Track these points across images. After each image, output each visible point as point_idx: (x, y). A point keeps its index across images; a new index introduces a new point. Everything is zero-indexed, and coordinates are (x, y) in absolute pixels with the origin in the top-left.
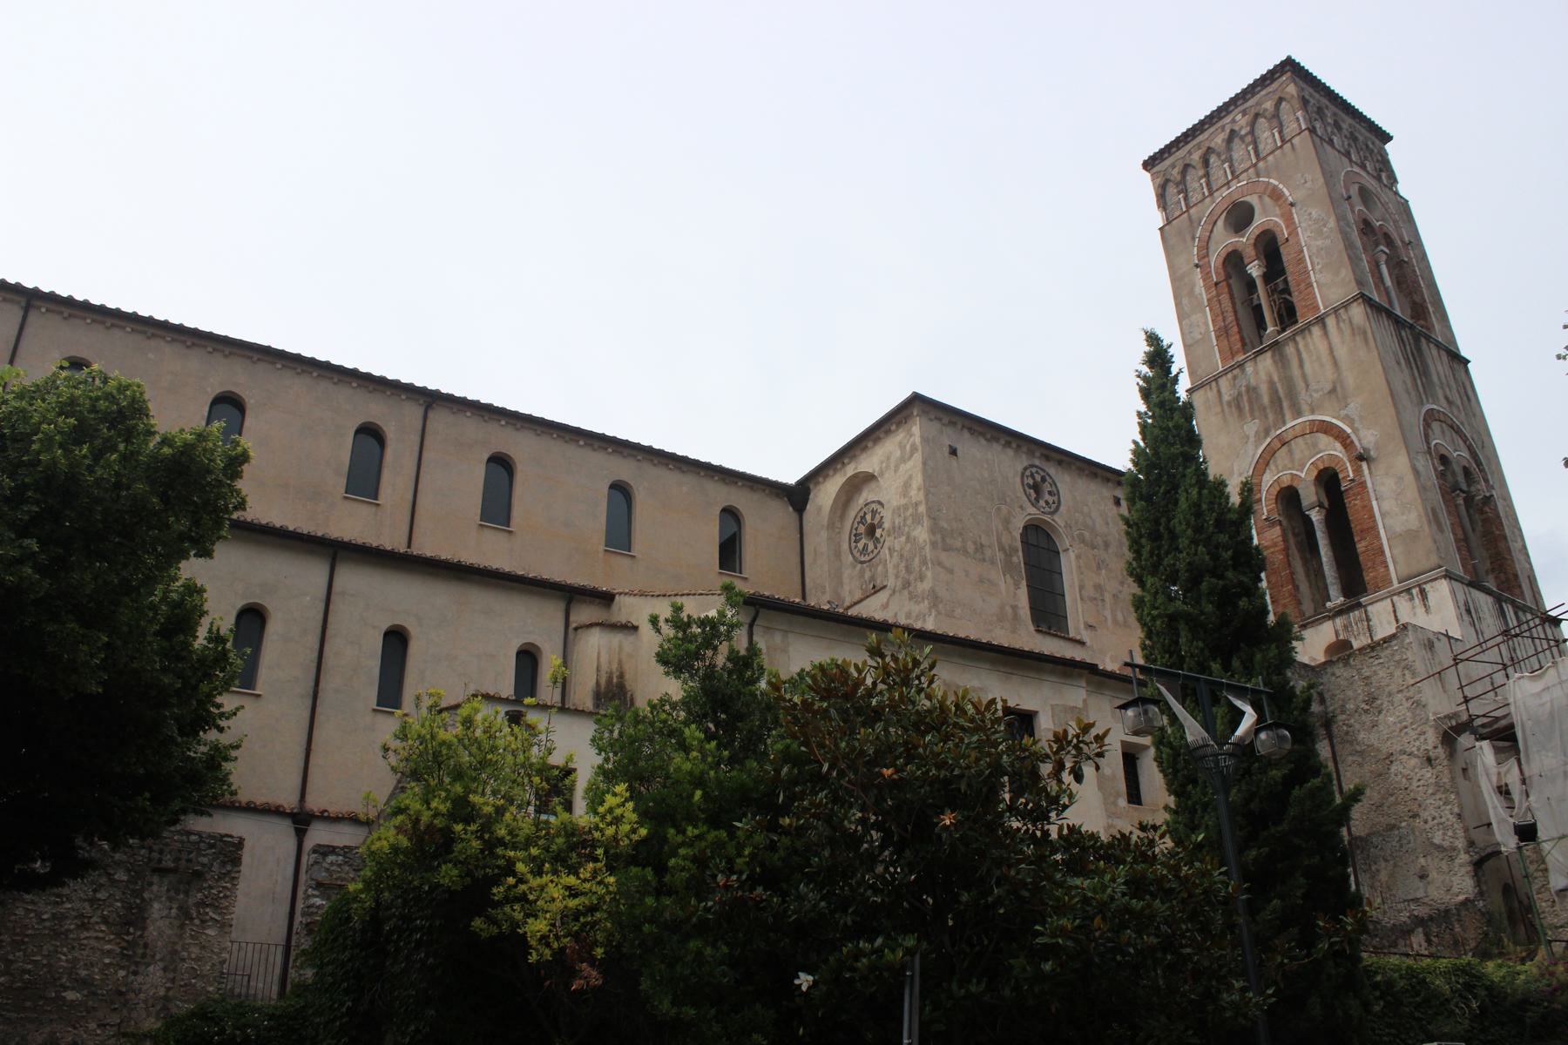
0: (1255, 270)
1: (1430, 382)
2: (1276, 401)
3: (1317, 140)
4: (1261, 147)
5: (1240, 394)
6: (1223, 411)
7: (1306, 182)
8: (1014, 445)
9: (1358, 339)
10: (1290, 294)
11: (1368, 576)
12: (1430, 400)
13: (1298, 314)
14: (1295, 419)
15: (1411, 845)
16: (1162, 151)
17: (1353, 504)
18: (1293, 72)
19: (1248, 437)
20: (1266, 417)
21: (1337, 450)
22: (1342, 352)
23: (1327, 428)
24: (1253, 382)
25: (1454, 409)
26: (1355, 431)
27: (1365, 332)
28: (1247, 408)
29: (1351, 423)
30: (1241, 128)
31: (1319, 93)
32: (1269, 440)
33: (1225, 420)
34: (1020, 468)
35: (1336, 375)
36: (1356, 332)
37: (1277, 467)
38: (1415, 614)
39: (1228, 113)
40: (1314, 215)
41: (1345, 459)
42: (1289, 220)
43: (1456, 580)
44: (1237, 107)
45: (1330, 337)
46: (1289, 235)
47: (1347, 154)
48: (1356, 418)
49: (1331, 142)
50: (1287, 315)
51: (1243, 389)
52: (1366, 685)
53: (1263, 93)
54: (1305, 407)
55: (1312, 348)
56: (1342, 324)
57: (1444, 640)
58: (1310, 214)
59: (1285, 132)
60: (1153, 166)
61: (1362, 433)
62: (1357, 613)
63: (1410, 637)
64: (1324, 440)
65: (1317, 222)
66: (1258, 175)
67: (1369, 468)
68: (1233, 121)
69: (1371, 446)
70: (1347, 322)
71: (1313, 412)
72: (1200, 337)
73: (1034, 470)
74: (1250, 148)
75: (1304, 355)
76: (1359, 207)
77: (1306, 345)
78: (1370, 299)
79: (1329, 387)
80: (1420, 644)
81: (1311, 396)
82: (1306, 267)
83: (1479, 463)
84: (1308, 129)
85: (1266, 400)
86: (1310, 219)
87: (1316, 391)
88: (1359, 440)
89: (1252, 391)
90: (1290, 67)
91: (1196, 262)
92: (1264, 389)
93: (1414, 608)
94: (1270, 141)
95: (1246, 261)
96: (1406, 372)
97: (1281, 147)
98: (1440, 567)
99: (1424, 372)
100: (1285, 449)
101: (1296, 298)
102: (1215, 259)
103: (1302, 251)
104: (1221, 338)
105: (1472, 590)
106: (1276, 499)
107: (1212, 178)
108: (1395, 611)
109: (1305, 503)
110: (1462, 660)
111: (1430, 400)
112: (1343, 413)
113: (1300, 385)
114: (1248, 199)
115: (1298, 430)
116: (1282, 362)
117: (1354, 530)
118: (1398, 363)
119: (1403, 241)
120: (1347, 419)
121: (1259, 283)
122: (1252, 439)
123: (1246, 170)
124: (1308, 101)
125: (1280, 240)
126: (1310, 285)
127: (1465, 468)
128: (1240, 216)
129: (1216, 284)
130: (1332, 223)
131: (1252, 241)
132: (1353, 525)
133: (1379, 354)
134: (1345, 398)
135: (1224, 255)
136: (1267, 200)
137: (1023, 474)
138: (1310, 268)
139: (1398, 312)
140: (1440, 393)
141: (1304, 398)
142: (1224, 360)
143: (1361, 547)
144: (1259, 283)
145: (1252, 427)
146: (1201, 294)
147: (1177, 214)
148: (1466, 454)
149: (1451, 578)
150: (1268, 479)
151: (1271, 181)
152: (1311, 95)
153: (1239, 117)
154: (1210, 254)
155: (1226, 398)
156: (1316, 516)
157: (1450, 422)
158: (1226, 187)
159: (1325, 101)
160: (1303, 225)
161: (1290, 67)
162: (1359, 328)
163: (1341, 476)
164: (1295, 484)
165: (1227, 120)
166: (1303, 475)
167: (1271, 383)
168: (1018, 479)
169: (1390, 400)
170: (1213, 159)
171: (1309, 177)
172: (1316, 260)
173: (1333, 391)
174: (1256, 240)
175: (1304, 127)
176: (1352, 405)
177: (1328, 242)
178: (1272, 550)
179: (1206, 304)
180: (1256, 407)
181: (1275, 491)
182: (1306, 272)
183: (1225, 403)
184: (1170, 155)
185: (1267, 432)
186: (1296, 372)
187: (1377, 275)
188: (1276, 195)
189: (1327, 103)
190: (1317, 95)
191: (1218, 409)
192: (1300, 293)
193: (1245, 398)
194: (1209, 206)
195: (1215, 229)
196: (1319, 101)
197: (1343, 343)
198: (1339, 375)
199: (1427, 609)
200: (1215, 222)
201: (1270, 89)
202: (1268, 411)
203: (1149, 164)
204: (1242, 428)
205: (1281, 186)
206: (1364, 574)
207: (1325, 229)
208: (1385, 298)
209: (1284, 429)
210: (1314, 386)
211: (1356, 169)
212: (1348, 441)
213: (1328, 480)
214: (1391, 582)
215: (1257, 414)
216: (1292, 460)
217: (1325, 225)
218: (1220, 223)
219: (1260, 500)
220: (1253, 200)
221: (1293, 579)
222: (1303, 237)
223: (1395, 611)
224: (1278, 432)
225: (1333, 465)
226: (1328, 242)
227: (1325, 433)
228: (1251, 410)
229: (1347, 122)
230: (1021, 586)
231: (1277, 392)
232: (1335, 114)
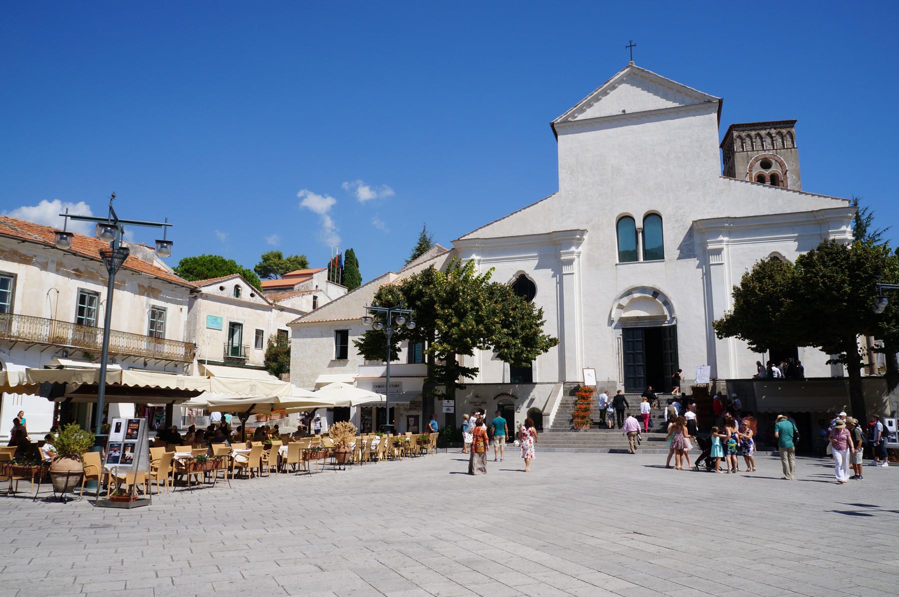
30: (773, 133)
65: (794, 180)
66: (777, 154)
102: (754, 174)
136: (778, 164)
158: (763, 151)
188: (782, 165)
194: (755, 155)
205: (784, 162)
220: (773, 161)
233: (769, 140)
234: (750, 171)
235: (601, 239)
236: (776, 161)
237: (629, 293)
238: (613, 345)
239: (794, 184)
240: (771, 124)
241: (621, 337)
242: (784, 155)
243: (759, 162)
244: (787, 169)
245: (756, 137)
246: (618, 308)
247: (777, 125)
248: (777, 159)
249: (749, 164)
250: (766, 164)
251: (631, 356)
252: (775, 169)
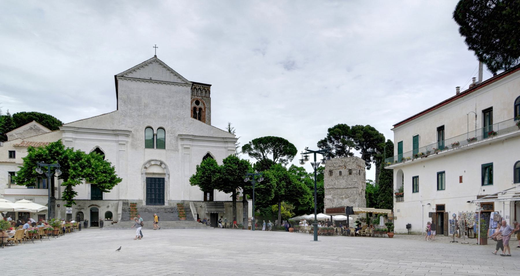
0: (198, 112)
4: (203, 94)
42: (205, 109)
53: (206, 86)
65: (208, 112)
68: (200, 86)
153: (201, 87)
165: (200, 85)
170: (195, 89)
188: (204, 105)
220: (201, 102)
233: (200, 92)
235: (138, 136)
237: (150, 161)
238: (142, 184)
241: (145, 181)
243: (195, 101)
245: (194, 90)
246: (145, 168)
247: (203, 85)
251: (149, 189)
252: (201, 105)
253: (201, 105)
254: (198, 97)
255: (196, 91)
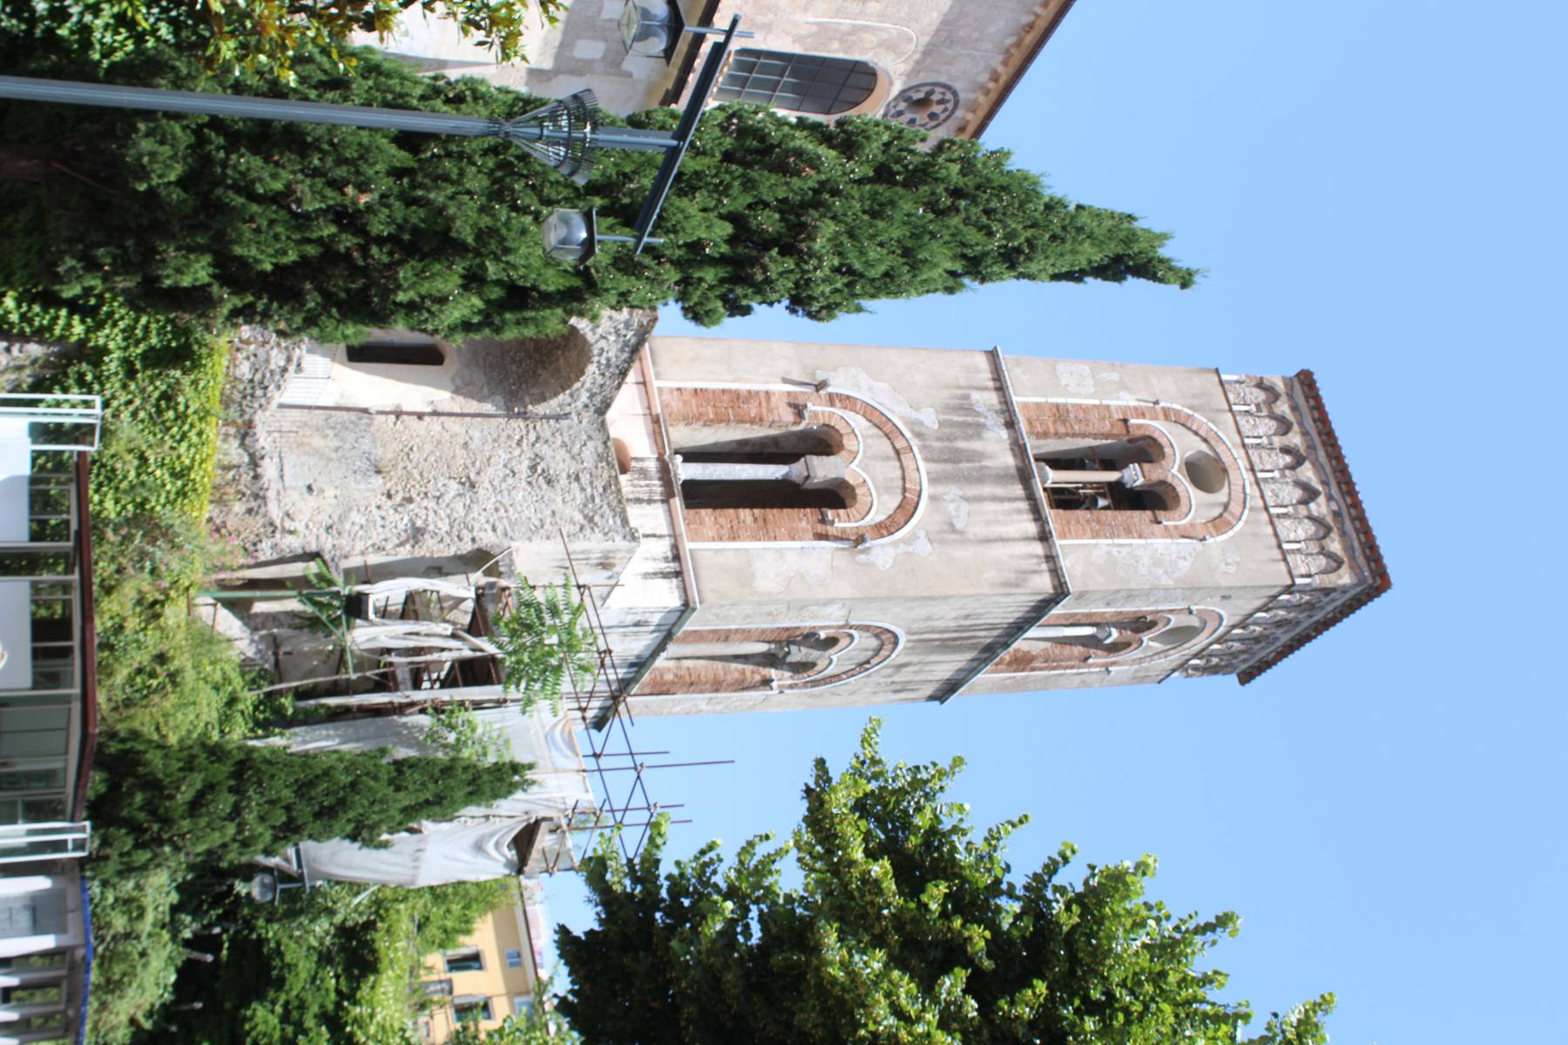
0: (1134, 476)
1: (933, 651)
2: (955, 457)
3: (1274, 592)
4: (1287, 523)
5: (978, 414)
6: (959, 387)
7: (1227, 564)
8: (991, 85)
9: (1012, 576)
10: (1088, 509)
11: (706, 514)
12: (911, 644)
13: (1061, 511)
14: (928, 473)
15: (353, 484)
16: (1317, 398)
17: (804, 518)
18: (1370, 587)
19: (917, 409)
20: (939, 439)
21: (875, 516)
22: (1000, 551)
23: (907, 509)
24: (987, 435)
25: (889, 671)
26: (895, 544)
27: (1017, 586)
28: (956, 418)
29: (907, 541)
31: (1333, 611)
32: (908, 435)
33: (947, 387)
34: (957, 86)
35: (971, 537)
36: (1022, 576)
37: (871, 437)
38: (647, 559)
39: (1343, 494)
40: (1182, 564)
41: (861, 523)
43: (680, 617)
44: (1348, 507)
45: (1022, 543)
46: (1166, 527)
47: (1243, 624)
48: (911, 549)
49: (1264, 608)
50: (1065, 499)
51: (982, 420)
52: (569, 476)
53: (1356, 544)
54: (940, 489)
55: (1015, 517)
56: (1035, 561)
57: (613, 582)
58: (1185, 559)
59: (1298, 557)
60: (1302, 383)
61: (891, 551)
62: (659, 489)
63: (620, 543)
64: (892, 502)
66: (1252, 509)
67: (843, 549)
69: (871, 557)
70: (1037, 568)
71: (933, 498)
72: (1063, 383)
73: (950, 106)
74: (1290, 509)
75: (1007, 506)
76: (1175, 621)
77: (1019, 511)
78: (1057, 603)
79: (959, 525)
80: (609, 551)
81: (952, 501)
82: (1119, 537)
83: (815, 683)
84: (1293, 584)
85: (961, 444)
86: (1178, 557)
87: (957, 510)
88: (883, 546)
89: (977, 430)
90: (1375, 582)
91: (1162, 404)
92: (976, 445)
93: (655, 560)
94: (1292, 537)
95: (1146, 466)
96: (953, 624)
97: (1280, 547)
98: (701, 603)
99: (947, 646)
100: (891, 453)
101: (1081, 514)
102: (1160, 428)
103: (1140, 537)
104: (1054, 410)
105: (664, 634)
106: (829, 426)
107: (1264, 454)
108: (654, 536)
109: (815, 461)
110: (582, 595)
111: (911, 644)
112: (922, 534)
113: (972, 491)
114: (1225, 490)
115: (911, 473)
116: (1001, 478)
117: (768, 511)
118: (967, 617)
119: (1113, 664)
120: (913, 538)
121: (1112, 476)
122: (914, 415)
123: (1262, 497)
124: (1327, 595)
125: (1161, 514)
126: (1095, 535)
127: (813, 665)
128: (1205, 472)
129: (1125, 421)
130: (1167, 581)
131: (1169, 480)
132: (775, 511)
133: (986, 596)
134: (942, 542)
135: (1163, 441)
136: (1217, 511)
137: (948, 88)
138: (1117, 541)
139: (1033, 632)
140: (915, 659)
141: (952, 491)
142: (1025, 406)
143: (745, 514)
144: (1112, 476)
145: (930, 419)
146: (1118, 398)
147: (1231, 397)
148: (831, 671)
149: (683, 612)
150: (858, 422)
151: (1241, 524)
152: (1333, 600)
154: (1168, 423)
155: (976, 396)
156: (795, 471)
157: (873, 662)
159: (1319, 616)
160: (1174, 548)
161: (1375, 582)
162: (1024, 580)
163: (842, 512)
164: (843, 453)
166: (853, 466)
167: (980, 456)
168: (943, 79)
169: (926, 594)
171: (1232, 569)
172: (1124, 551)
173: (952, 528)
174: (1170, 485)
175: (1299, 581)
176: (929, 547)
177: (1143, 571)
178: (764, 405)
179: (1105, 402)
180: (955, 430)
181: (840, 427)
182: (1112, 536)
183: (968, 392)
184: (1312, 409)
185: (919, 435)
186: (988, 490)
187: (1083, 621)
188: (1219, 523)
189: (1315, 618)
190: (1330, 608)
191: (962, 382)
192: (1088, 521)
193: (970, 419)
194: (1230, 438)
195: (1198, 439)
196: (1322, 608)
197: (1012, 556)
198: (969, 541)
199: (646, 575)
200: (1205, 440)
201: (1358, 553)
202: (947, 444)
203: (1306, 381)
204: (931, 406)
205: (1231, 533)
206: (709, 511)
207: (1161, 572)
208: (1052, 622)
209: (918, 457)
210: (965, 507)
211: (1221, 630)
212: (884, 532)
213: (835, 496)
214: (692, 540)
215: (947, 430)
216: (875, 458)
217: (1166, 572)
218: (1204, 447)
219: (832, 404)
220: (1221, 496)
221: (720, 421)
222: (1160, 544)
223: (654, 536)
224: (916, 449)
225: (857, 506)
226: (1143, 571)
227: (900, 506)
228: (952, 424)
229: (1284, 638)
230: (797, 45)
231: (968, 461)
232: (1298, 623)
234: (1166, 414)
236: (1226, 506)
239: (1157, 563)
240: (1349, 500)
242: (1255, 535)
244: (1210, 540)
247: (1353, 520)
248: (1235, 508)
249: (1190, 412)
250: (1205, 472)
252: (1196, 503)
253: (1196, 503)
254: (1248, 477)
255: (1281, 463)
